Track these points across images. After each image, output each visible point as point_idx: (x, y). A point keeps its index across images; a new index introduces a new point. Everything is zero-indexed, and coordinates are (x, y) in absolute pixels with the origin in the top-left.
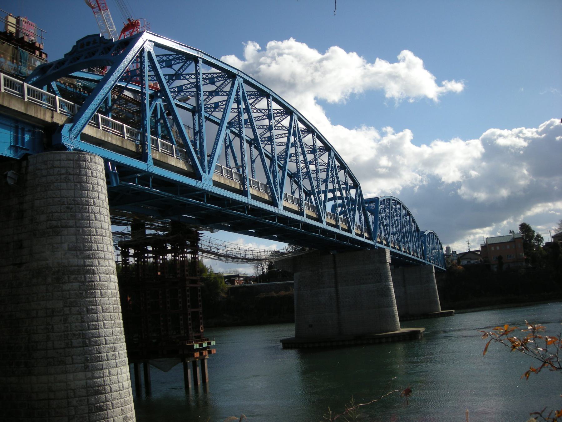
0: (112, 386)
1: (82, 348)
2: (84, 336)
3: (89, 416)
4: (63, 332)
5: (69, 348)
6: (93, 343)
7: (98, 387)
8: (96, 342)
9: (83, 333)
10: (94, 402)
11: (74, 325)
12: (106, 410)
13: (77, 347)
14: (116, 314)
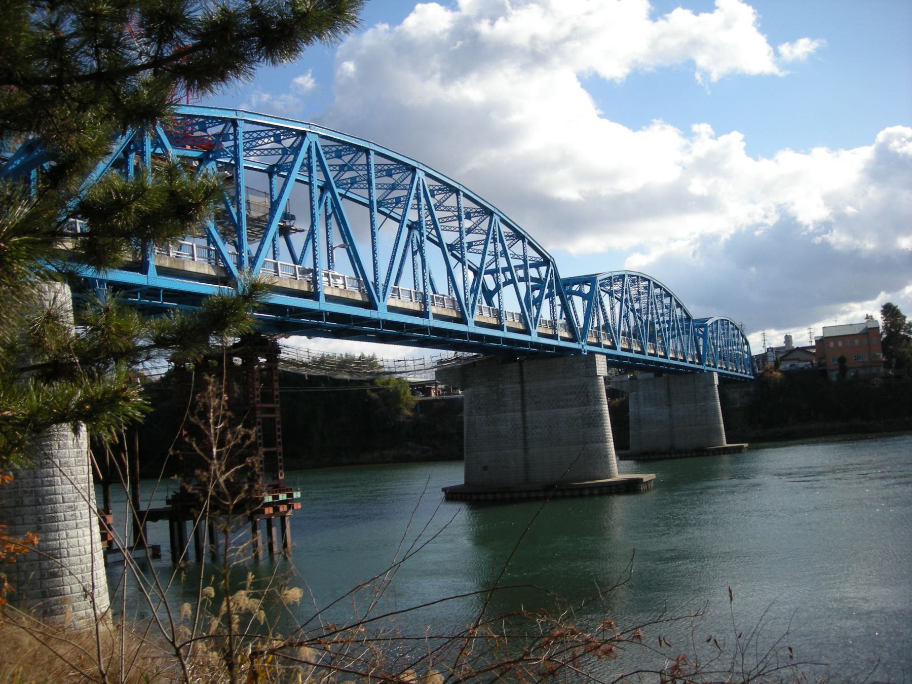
0: (71, 550)
1: (34, 507)
2: (37, 494)
3: (41, 583)
4: (13, 489)
5: (19, 506)
6: (47, 502)
7: (52, 550)
8: (51, 500)
9: (36, 491)
10: (47, 567)
11: (25, 481)
12: (62, 576)
13: (29, 506)
14: (80, 468)
